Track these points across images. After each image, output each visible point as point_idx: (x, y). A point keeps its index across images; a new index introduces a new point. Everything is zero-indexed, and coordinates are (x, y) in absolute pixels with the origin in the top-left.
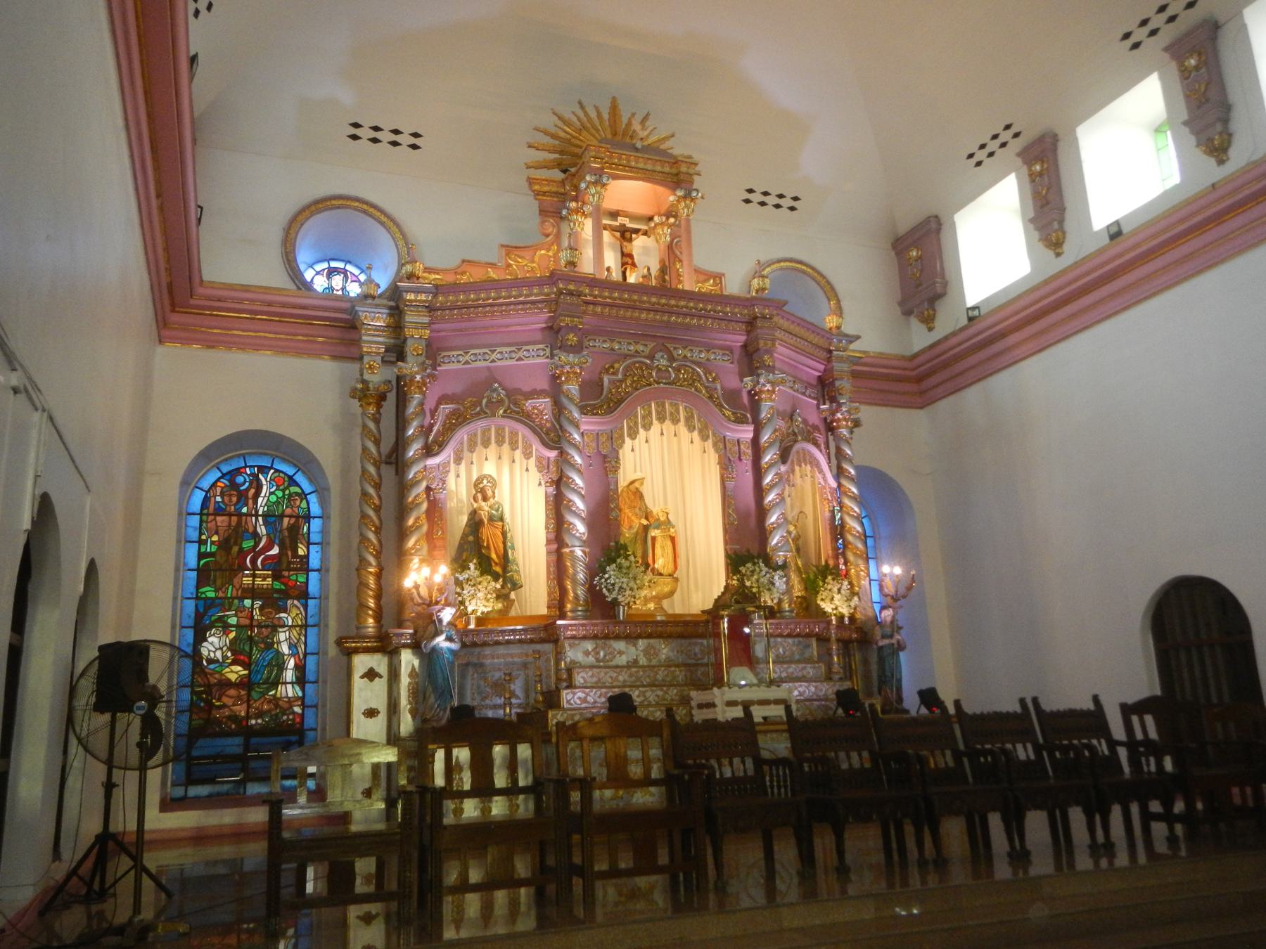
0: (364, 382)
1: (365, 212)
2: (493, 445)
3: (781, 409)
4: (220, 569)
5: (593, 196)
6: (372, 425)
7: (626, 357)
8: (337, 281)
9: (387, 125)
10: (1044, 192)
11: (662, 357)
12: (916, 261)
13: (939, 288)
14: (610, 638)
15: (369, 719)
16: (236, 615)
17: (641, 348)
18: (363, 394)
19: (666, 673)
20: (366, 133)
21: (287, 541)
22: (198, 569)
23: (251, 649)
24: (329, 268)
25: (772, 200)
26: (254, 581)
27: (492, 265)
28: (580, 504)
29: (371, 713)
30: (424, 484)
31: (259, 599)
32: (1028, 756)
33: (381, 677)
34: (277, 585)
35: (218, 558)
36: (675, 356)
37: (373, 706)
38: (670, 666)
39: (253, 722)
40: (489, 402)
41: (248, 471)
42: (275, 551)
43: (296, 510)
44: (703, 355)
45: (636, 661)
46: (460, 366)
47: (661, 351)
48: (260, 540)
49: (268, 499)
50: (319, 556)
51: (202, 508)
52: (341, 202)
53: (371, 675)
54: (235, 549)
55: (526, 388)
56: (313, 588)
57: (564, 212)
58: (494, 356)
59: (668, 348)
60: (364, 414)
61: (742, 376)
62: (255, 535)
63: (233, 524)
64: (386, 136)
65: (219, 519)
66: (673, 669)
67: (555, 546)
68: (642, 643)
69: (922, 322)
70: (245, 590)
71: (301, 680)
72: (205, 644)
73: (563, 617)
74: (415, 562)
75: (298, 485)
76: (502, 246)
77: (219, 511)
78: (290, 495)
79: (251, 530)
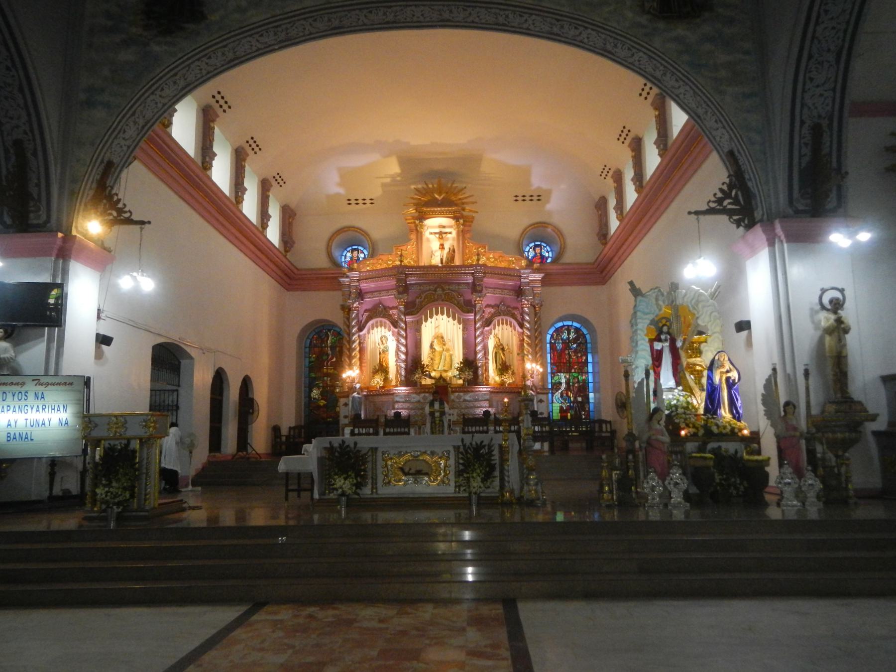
1: (356, 231)
2: (379, 327)
3: (493, 304)
6: (346, 320)
8: (355, 253)
17: (431, 287)
20: (353, 202)
22: (309, 367)
25: (527, 198)
28: (403, 349)
30: (358, 342)
34: (336, 372)
39: (329, 420)
42: (334, 360)
45: (419, 401)
55: (391, 306)
61: (472, 293)
62: (327, 355)
65: (315, 349)
73: (397, 386)
74: (355, 368)
77: (315, 346)
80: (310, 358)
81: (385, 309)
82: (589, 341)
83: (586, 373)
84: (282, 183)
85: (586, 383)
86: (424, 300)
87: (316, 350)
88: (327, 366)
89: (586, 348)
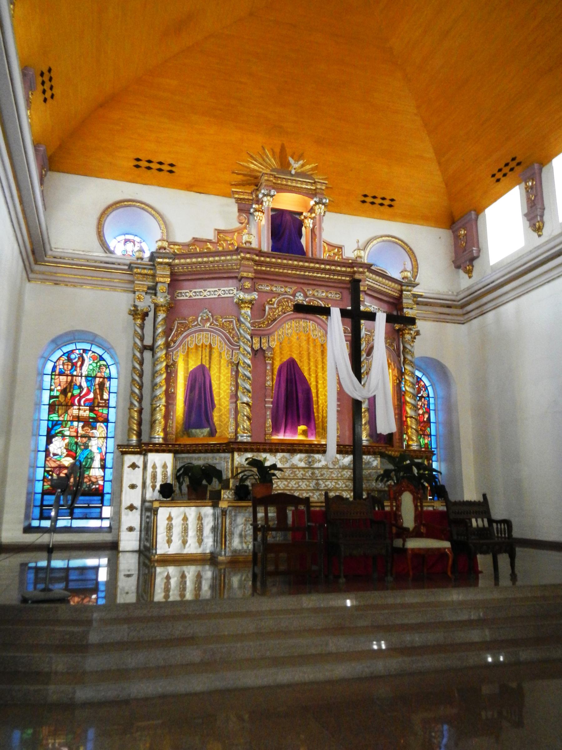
0: (135, 306)
1: (143, 209)
4: (61, 404)
5: (266, 202)
6: (139, 330)
7: (279, 295)
8: (129, 246)
9: (155, 160)
10: (533, 198)
11: (300, 295)
12: (463, 237)
13: (475, 255)
14: (261, 452)
15: (132, 490)
16: (69, 430)
17: (288, 290)
18: (135, 312)
19: (291, 471)
20: (144, 164)
21: (98, 391)
22: (49, 405)
23: (77, 449)
24: (125, 239)
25: (378, 201)
26: (79, 412)
27: (210, 241)
29: (133, 487)
30: (164, 364)
31: (82, 421)
32: (484, 525)
33: (139, 467)
34: (92, 415)
35: (60, 399)
36: (308, 294)
37: (134, 483)
38: (294, 468)
40: (202, 319)
41: (77, 351)
42: (91, 396)
43: (103, 374)
44: (324, 294)
46: (187, 298)
47: (299, 292)
48: (83, 389)
49: (88, 368)
50: (115, 399)
51: (52, 372)
52: (129, 203)
53: (134, 466)
54: (69, 394)
56: (112, 418)
57: (252, 210)
58: (205, 293)
59: (302, 289)
60: (135, 324)
62: (80, 387)
63: (69, 380)
64: (154, 166)
65: (61, 377)
66: (295, 470)
67: (234, 400)
68: (280, 455)
69: (466, 273)
70: (73, 417)
71: (103, 467)
72: (51, 445)
75: (104, 360)
76: (216, 230)
77: (61, 374)
78: (100, 366)
79: (78, 384)
80: (51, 390)
81: (212, 316)
82: (431, 395)
83: (428, 435)
84: (48, 94)
85: (428, 448)
86: (278, 308)
87: (63, 379)
88: (80, 405)
89: (429, 404)
